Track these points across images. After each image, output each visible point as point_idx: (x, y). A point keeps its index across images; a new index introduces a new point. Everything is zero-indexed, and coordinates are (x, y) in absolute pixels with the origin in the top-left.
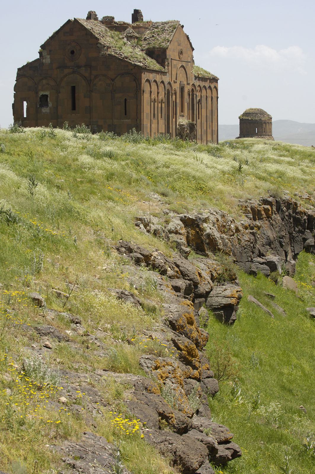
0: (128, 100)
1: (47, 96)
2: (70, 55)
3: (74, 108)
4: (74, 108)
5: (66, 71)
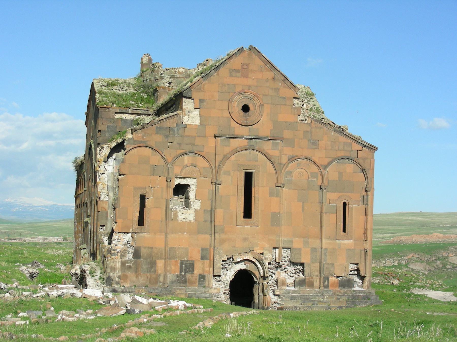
0: (350, 206)
2: (242, 113)
3: (248, 213)
4: (248, 213)
5: (235, 143)
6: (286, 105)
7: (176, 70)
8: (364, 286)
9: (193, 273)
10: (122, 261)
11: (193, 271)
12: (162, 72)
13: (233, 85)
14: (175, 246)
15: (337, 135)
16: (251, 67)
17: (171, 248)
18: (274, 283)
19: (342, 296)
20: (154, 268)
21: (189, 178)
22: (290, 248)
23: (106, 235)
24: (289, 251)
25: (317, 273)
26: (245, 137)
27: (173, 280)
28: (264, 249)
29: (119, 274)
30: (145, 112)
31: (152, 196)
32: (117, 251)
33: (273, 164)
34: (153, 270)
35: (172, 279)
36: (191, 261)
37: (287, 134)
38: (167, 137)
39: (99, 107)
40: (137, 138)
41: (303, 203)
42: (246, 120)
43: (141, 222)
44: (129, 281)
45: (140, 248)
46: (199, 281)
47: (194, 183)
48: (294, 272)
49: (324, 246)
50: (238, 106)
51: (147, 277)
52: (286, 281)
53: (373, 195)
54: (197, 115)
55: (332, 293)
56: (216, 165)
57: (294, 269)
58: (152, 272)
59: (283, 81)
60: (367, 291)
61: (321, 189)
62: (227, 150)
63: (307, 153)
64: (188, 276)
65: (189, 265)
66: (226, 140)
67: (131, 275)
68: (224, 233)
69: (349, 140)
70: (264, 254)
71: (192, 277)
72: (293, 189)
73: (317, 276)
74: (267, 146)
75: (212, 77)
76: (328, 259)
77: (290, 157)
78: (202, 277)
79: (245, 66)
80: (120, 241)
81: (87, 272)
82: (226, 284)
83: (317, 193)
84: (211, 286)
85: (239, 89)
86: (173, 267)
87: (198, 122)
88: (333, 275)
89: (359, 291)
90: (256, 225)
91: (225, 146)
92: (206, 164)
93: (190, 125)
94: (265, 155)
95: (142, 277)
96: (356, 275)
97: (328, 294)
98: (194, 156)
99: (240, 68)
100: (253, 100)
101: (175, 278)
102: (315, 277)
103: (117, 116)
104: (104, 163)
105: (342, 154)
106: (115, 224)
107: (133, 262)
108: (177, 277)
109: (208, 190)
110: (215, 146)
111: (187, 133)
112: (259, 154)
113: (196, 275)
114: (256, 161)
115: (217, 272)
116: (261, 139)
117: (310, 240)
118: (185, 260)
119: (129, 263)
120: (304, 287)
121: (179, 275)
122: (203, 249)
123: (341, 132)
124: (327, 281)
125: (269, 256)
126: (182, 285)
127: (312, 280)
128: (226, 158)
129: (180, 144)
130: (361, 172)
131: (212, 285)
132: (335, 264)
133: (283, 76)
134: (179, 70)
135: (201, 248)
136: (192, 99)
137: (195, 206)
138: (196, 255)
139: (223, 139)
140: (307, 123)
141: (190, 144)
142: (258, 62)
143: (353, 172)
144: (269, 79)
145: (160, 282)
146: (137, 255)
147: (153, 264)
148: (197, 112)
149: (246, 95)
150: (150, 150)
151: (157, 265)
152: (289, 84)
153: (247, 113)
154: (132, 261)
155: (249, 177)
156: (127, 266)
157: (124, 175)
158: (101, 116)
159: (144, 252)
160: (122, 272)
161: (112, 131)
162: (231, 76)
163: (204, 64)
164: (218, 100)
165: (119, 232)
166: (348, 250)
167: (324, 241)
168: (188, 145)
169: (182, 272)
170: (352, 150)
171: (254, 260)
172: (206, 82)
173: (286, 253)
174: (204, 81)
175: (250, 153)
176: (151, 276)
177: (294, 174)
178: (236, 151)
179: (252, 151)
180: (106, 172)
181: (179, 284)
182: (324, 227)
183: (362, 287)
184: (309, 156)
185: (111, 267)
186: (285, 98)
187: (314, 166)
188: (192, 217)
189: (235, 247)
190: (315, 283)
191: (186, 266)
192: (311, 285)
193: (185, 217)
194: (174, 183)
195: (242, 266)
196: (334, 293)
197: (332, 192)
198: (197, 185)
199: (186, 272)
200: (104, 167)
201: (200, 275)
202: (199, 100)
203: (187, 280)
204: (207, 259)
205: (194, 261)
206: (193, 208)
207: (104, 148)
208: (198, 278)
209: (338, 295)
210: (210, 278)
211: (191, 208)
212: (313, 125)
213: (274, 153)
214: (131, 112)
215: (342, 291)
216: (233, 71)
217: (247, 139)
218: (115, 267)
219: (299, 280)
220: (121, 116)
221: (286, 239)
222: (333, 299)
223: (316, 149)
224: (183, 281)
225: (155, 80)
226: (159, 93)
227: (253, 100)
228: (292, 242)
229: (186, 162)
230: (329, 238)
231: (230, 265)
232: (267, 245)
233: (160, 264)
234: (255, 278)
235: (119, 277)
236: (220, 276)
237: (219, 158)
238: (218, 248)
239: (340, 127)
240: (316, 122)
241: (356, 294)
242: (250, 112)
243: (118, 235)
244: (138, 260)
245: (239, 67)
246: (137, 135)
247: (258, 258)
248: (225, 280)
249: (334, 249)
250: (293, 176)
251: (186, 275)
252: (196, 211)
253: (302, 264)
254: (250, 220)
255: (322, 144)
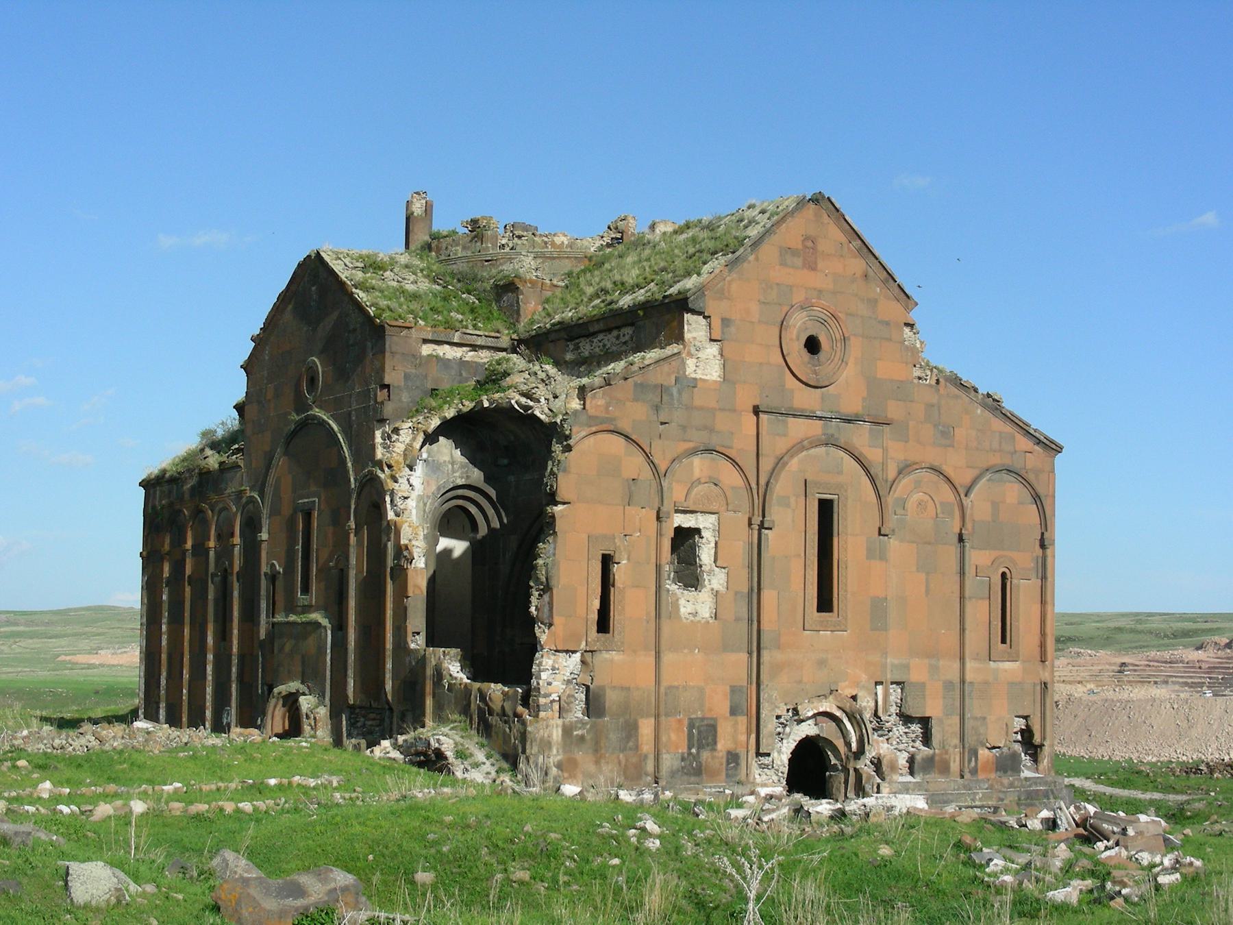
1: (697, 531)
3: (825, 603)
4: (825, 603)
5: (799, 428)
6: (891, 340)
7: (546, 239)
8: (1041, 767)
9: (715, 750)
10: (564, 722)
11: (715, 743)
12: (504, 242)
13: (787, 286)
14: (676, 684)
15: (987, 414)
16: (823, 246)
17: (670, 687)
18: (869, 767)
19: (1008, 794)
20: (633, 740)
21: (701, 512)
22: (904, 683)
23: (454, 656)
24: (899, 690)
25: (956, 741)
26: (819, 413)
27: (674, 768)
28: (857, 684)
29: (559, 758)
30: (490, 342)
31: (626, 556)
32: (551, 699)
33: (873, 480)
34: (631, 744)
35: (672, 766)
36: (712, 719)
37: (894, 410)
38: (657, 408)
39: (386, 325)
40: (594, 410)
41: (927, 574)
42: (815, 373)
43: (603, 624)
44: (581, 776)
45: (602, 688)
46: (727, 770)
47: (711, 526)
48: (904, 739)
49: (969, 677)
50: (798, 339)
51: (620, 763)
52: (897, 761)
53: (1054, 556)
54: (714, 356)
55: (986, 786)
56: (760, 482)
57: (906, 733)
58: (631, 749)
59: (884, 282)
60: (1050, 779)
61: (961, 539)
62: (782, 445)
63: (932, 455)
64: (705, 757)
65: (705, 728)
66: (779, 420)
67: (583, 757)
68: (779, 648)
69: (1008, 428)
70: (858, 697)
71: (713, 758)
72: (908, 542)
73: (955, 747)
74: (860, 437)
75: (745, 264)
76: (975, 708)
77: (902, 466)
78: (733, 757)
79: (810, 242)
80: (557, 672)
81: (449, 754)
82: (780, 774)
83: (953, 550)
84: (751, 779)
85: (799, 297)
86: (673, 736)
87: (718, 374)
88: (983, 745)
89: (1035, 781)
90: (843, 627)
91: (778, 434)
92: (730, 477)
93: (704, 381)
94: (858, 460)
95: (608, 763)
96: (1019, 742)
97: (980, 788)
98: (713, 459)
99: (800, 247)
100: (827, 326)
101: (677, 764)
102: (951, 750)
103: (426, 350)
104: (407, 469)
105: (996, 460)
106: (546, 631)
107: (588, 726)
108: (683, 759)
109: (742, 543)
110: (755, 433)
111: (698, 402)
112: (846, 457)
113: (721, 754)
114: (840, 473)
115: (768, 745)
116: (849, 421)
117: (941, 663)
118: (697, 718)
119: (580, 728)
120: (933, 775)
121: (686, 755)
122: (734, 690)
123: (997, 409)
124: (973, 759)
125: (868, 702)
126: (693, 779)
127: (947, 757)
128: (780, 462)
129: (684, 428)
130: (1032, 503)
131: (755, 778)
132: (988, 717)
133: (885, 269)
134: (556, 239)
135: (731, 686)
136: (704, 317)
137: (713, 581)
138: (719, 705)
139: (772, 417)
140: (930, 385)
141: (705, 428)
142: (835, 233)
143: (1019, 504)
144: (856, 275)
145: (647, 775)
146: (594, 704)
147: (631, 730)
148: (714, 349)
149: (813, 313)
150: (622, 440)
151: (640, 730)
152: (897, 290)
153: (816, 357)
154: (587, 723)
155: (826, 509)
156: (577, 735)
157: (564, 503)
158: (390, 347)
159: (612, 699)
160: (565, 752)
161: (417, 387)
162: (783, 264)
163: (616, 228)
164: (759, 321)
165: (556, 651)
166: (1011, 684)
167: (969, 665)
168: (700, 430)
169: (693, 746)
170: (1016, 451)
171: (838, 713)
172: (734, 275)
173: (895, 693)
174: (730, 271)
175: (828, 454)
176: (627, 760)
177: (909, 505)
178: (799, 447)
179: (832, 449)
180: (414, 495)
181: (685, 778)
182: (967, 632)
183: (1037, 770)
184: (936, 464)
185: (542, 739)
186: (887, 324)
187: (946, 487)
188: (707, 610)
189: (800, 682)
190: (952, 764)
191: (699, 732)
192: (945, 769)
193: (694, 611)
194: (673, 523)
195: (808, 729)
196: (991, 787)
197: (980, 549)
198: (718, 531)
199: (700, 748)
200: (408, 480)
201: (729, 753)
202: (720, 320)
203: (703, 768)
204: (742, 714)
205: (715, 720)
206: (708, 586)
207: (401, 432)
208: (724, 760)
209: (1000, 791)
210: (749, 760)
211: (705, 586)
212: (942, 391)
213: (873, 455)
214: (458, 341)
215: (1006, 781)
216: (787, 251)
217: (820, 418)
218: (551, 739)
219: (923, 759)
220: (434, 350)
221: (896, 662)
222: (992, 801)
223: (949, 446)
224: (693, 768)
225: (487, 261)
226: (523, 294)
227: (827, 326)
228: (907, 667)
229: (697, 473)
230: (976, 658)
231: (786, 725)
232: (864, 677)
233: (646, 728)
234: (832, 757)
235: (559, 766)
236: (769, 755)
237: (766, 464)
238: (767, 685)
239: (989, 396)
240: (948, 384)
241: (1030, 786)
242: (822, 355)
243: (553, 657)
244: (600, 720)
245: (797, 244)
246: (594, 402)
247: (850, 707)
248: (779, 763)
249: (986, 683)
250: (907, 511)
251: (701, 754)
252: (716, 594)
253: (925, 722)
254: (830, 617)
255: (960, 433)
